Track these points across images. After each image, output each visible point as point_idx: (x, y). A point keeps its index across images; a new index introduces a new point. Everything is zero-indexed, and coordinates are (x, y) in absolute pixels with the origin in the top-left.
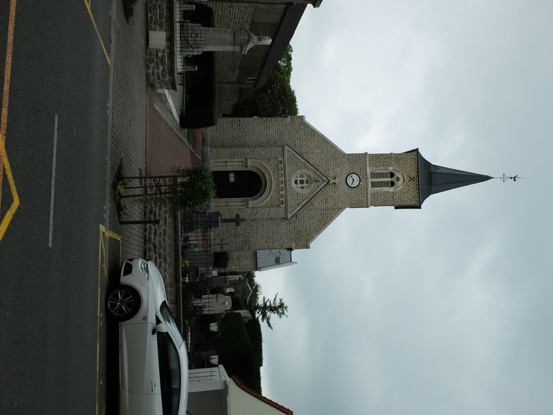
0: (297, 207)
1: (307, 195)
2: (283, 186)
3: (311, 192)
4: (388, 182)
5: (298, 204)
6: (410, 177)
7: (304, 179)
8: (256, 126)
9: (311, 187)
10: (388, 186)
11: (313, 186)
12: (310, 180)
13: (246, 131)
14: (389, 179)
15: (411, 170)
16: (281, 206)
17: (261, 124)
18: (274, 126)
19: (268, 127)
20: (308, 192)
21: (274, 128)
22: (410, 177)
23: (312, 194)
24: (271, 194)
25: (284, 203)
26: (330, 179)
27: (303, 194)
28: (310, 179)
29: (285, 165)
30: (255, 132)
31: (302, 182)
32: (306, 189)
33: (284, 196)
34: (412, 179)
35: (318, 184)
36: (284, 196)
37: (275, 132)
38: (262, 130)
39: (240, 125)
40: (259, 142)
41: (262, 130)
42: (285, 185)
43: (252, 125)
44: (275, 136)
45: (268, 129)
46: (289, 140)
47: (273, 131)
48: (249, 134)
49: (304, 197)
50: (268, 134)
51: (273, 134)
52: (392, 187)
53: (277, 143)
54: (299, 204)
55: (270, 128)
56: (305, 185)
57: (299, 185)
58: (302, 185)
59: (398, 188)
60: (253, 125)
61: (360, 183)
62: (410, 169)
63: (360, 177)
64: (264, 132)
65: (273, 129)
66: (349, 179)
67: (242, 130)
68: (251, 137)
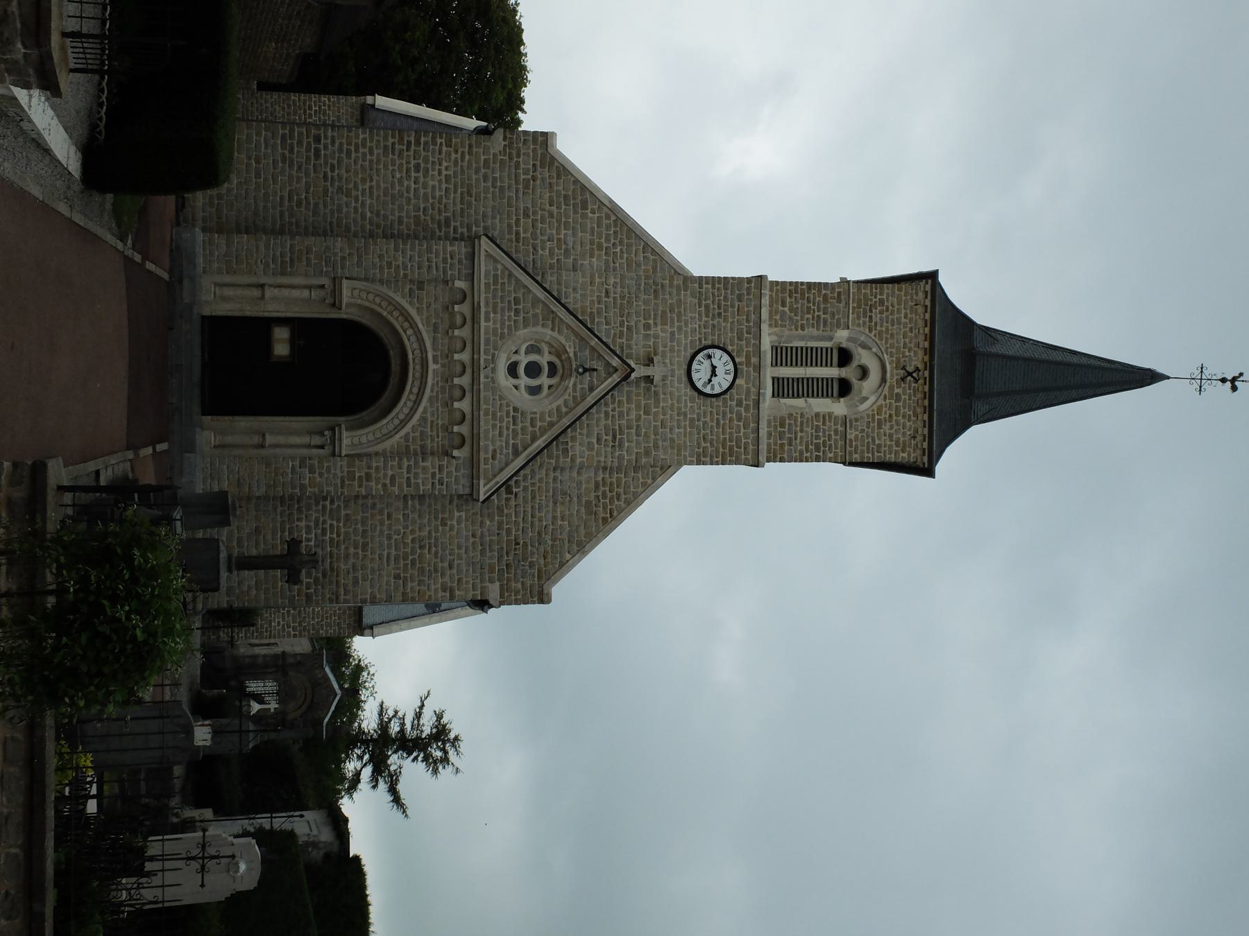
0: (512, 460)
1: (548, 419)
2: (465, 381)
3: (566, 406)
4: (829, 381)
5: (515, 446)
6: (904, 368)
7: (544, 360)
8: (378, 161)
9: (567, 388)
10: (827, 396)
11: (571, 385)
12: (563, 367)
13: (340, 178)
14: (833, 372)
15: (910, 343)
16: (456, 453)
17: (397, 152)
18: (445, 164)
19: (422, 165)
20: (554, 405)
21: (444, 173)
22: (904, 368)
23: (567, 413)
24: (421, 409)
25: (468, 441)
26: (633, 365)
27: (535, 413)
28: (561, 361)
29: (475, 310)
30: (374, 183)
31: (533, 370)
32: (548, 395)
33: (468, 417)
34: (910, 374)
35: (591, 381)
36: (468, 417)
37: (444, 186)
38: (398, 175)
39: (317, 151)
40: (385, 217)
41: (398, 175)
42: (475, 380)
43: (364, 155)
44: (444, 200)
45: (421, 174)
46: (494, 218)
47: (440, 182)
48: (351, 186)
49: (539, 424)
50: (422, 191)
51: (438, 194)
52: (842, 400)
53: (453, 224)
54: (520, 449)
55: (427, 170)
56: (544, 380)
57: (524, 380)
58: (534, 382)
59: (862, 403)
60: (368, 157)
61: (738, 381)
62: (907, 340)
63: (737, 360)
64: (406, 183)
65: (440, 173)
66: (698, 367)
67: (325, 173)
68: (357, 200)
